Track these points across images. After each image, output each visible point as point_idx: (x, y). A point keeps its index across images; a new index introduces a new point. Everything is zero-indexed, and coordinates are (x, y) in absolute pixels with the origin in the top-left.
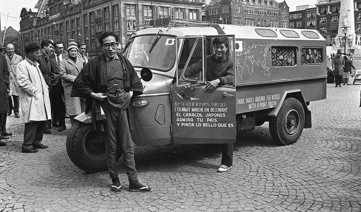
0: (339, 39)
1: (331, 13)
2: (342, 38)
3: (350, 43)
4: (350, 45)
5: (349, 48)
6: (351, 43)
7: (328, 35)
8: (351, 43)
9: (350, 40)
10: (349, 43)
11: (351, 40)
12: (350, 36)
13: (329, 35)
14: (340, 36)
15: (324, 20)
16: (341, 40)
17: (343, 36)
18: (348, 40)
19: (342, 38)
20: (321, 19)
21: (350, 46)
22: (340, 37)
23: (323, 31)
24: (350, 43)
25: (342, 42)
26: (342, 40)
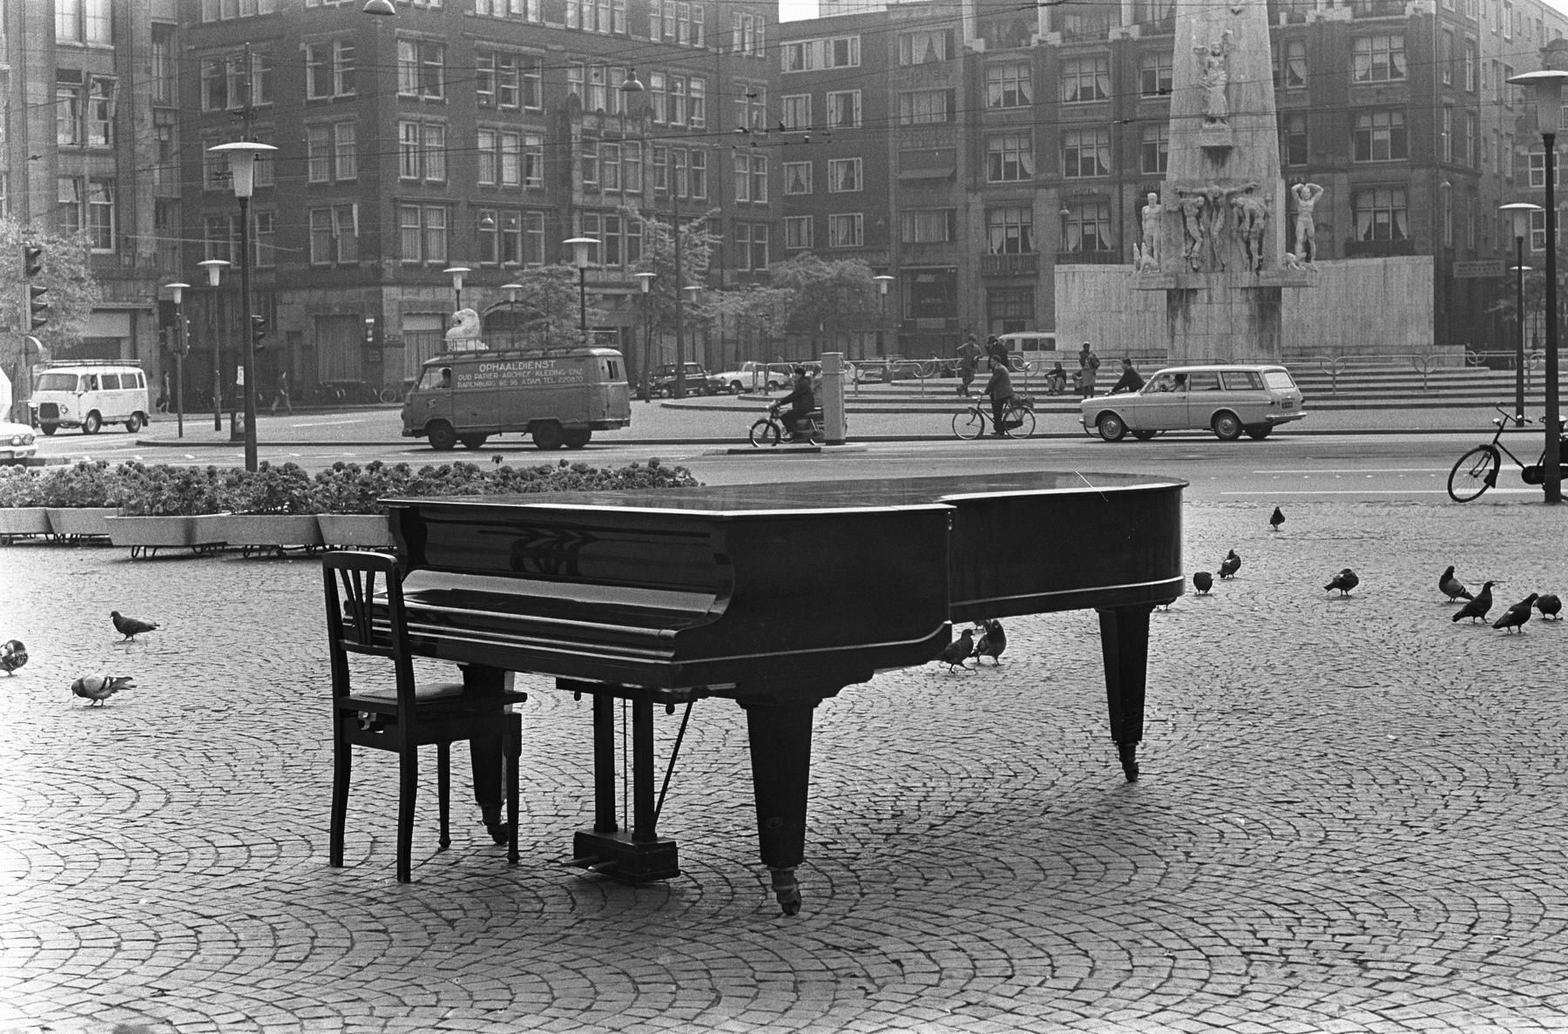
0: (1181, 210)
1: (1055, 39)
2: (1200, 209)
3: (1254, 245)
4: (1256, 257)
5: (1247, 279)
6: (1260, 243)
7: (1042, 192)
8: (1260, 243)
9: (1252, 219)
10: (1248, 243)
11: (1259, 221)
12: (1249, 191)
13: (1053, 191)
14: (1180, 188)
15: (1013, 87)
16: (1191, 220)
17: (1205, 190)
18: (1241, 220)
19: (1200, 209)
20: (994, 75)
21: (1255, 265)
22: (1181, 194)
23: (1010, 158)
24: (1254, 245)
25: (1196, 235)
26: (1198, 217)
